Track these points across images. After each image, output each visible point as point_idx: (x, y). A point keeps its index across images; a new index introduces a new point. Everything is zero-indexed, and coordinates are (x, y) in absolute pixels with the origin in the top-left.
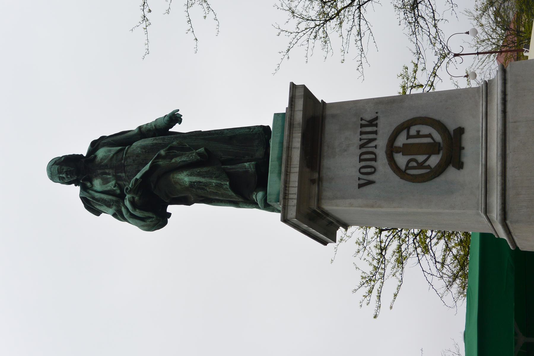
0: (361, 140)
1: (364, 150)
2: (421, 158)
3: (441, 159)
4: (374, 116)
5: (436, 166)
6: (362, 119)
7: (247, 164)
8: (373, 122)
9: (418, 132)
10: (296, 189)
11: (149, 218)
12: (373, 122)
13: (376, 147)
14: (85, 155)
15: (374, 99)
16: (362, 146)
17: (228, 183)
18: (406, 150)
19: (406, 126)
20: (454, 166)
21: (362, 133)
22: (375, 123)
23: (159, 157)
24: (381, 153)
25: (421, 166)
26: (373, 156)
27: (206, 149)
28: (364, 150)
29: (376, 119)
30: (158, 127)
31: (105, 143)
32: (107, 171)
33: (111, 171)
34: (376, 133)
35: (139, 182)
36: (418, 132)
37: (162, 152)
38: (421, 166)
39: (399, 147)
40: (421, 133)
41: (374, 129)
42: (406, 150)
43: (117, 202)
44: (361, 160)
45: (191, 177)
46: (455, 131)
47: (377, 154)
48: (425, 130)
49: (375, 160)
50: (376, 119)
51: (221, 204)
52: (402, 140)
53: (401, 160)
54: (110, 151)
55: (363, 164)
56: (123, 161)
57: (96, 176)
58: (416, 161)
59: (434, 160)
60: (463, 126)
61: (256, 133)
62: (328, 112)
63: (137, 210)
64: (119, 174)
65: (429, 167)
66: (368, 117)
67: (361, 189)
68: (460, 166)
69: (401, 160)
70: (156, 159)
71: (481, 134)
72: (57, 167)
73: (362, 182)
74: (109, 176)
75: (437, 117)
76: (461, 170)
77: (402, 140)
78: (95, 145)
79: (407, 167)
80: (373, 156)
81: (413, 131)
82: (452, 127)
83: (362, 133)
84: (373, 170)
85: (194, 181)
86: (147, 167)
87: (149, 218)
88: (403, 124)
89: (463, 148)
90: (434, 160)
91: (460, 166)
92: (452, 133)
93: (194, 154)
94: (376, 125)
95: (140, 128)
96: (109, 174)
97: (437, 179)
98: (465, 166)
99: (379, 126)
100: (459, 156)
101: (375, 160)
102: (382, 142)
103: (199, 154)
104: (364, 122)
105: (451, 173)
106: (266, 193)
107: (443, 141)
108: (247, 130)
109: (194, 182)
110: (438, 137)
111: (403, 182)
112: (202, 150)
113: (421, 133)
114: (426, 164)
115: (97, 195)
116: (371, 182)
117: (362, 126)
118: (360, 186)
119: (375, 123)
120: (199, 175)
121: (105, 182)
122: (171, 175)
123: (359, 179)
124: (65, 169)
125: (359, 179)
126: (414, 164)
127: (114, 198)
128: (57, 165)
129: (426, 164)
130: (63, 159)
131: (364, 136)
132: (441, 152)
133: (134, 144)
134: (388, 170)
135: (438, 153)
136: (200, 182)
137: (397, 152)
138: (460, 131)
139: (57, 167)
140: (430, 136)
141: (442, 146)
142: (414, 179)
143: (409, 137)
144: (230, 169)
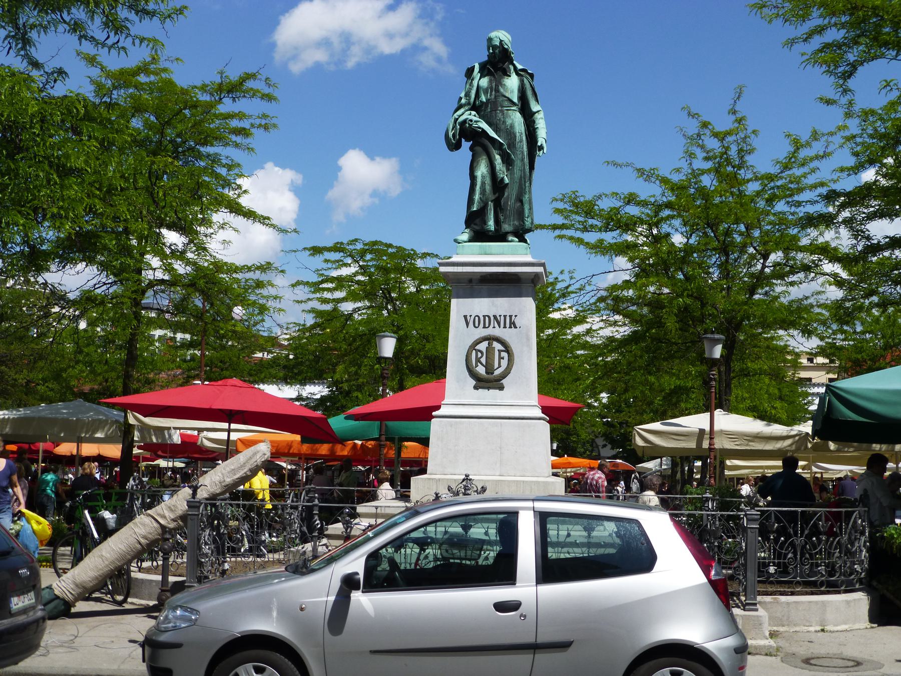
1: (492, 318)
2: (483, 360)
3: (481, 374)
6: (516, 316)
8: (513, 325)
12: (513, 325)
16: (495, 317)
18: (490, 349)
19: (507, 349)
21: (505, 316)
24: (489, 332)
25: (478, 360)
26: (487, 326)
28: (492, 318)
29: (516, 327)
30: (537, 130)
32: (494, 92)
33: (493, 97)
34: (505, 327)
36: (503, 358)
38: (478, 360)
41: (508, 325)
42: (490, 349)
43: (469, 104)
44: (484, 316)
48: (504, 363)
49: (484, 327)
50: (516, 327)
52: (497, 346)
53: (483, 346)
54: (512, 92)
59: (481, 370)
65: (477, 366)
66: (518, 322)
68: (476, 388)
69: (483, 346)
71: (499, 402)
73: (468, 318)
80: (487, 326)
81: (504, 354)
86: (493, 134)
90: (481, 370)
93: (502, 176)
94: (510, 327)
96: (491, 95)
101: (484, 327)
102: (497, 332)
103: (503, 179)
104: (513, 318)
110: (497, 372)
112: (507, 180)
115: (475, 83)
117: (511, 316)
118: (465, 317)
120: (483, 184)
122: (484, 157)
123: (471, 316)
126: (479, 355)
131: (502, 318)
138: (501, 388)
140: (500, 366)
143: (500, 351)
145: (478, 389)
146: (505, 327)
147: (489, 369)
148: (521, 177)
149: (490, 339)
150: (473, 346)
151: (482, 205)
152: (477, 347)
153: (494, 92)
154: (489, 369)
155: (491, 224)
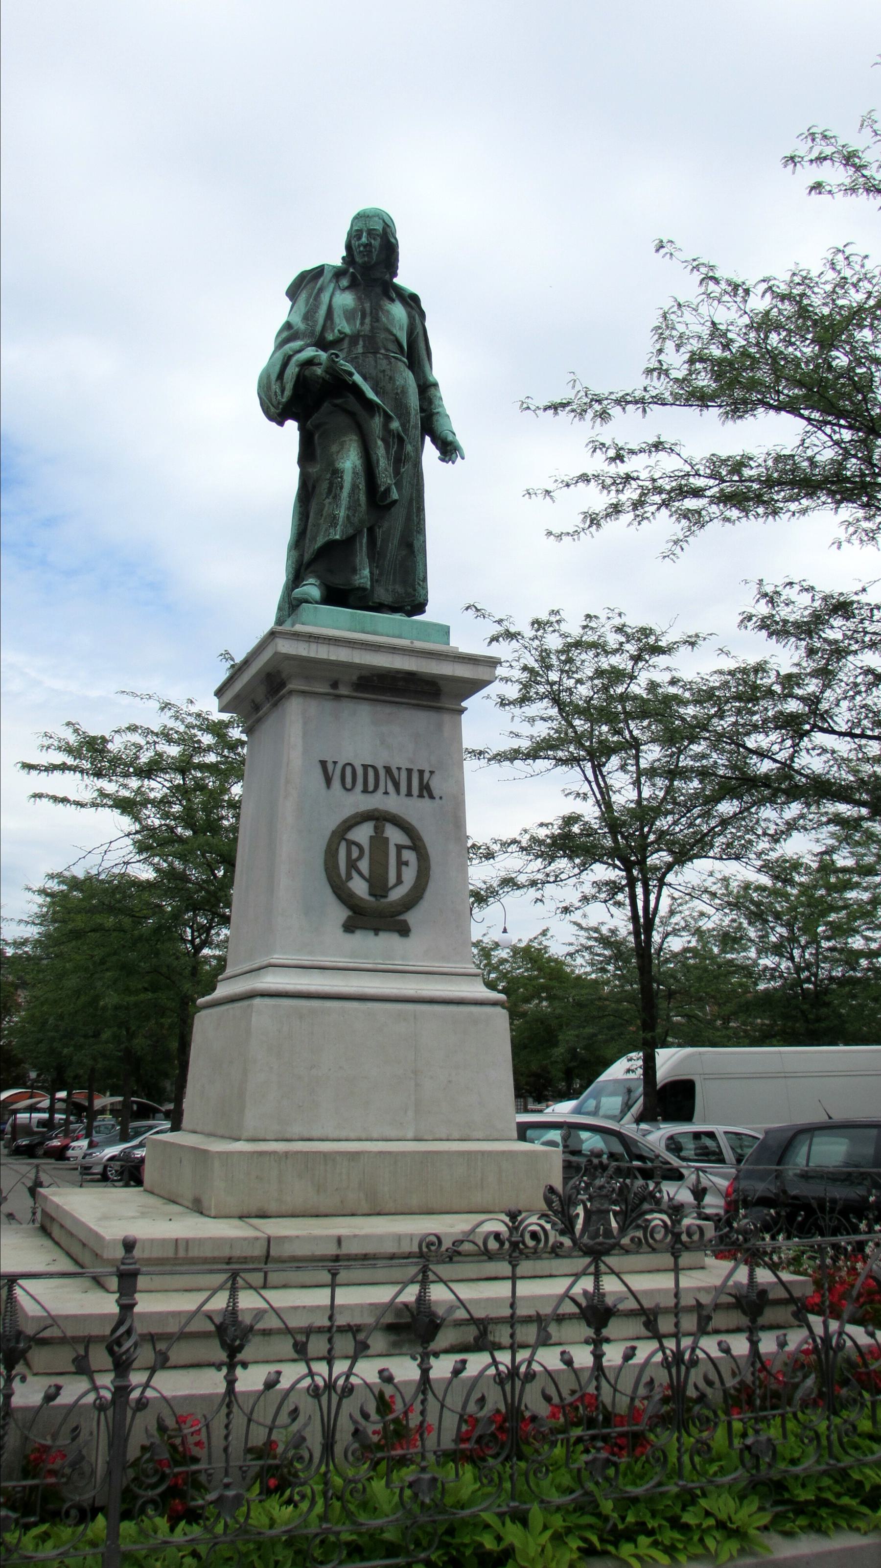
0: (399, 769)
1: (382, 773)
2: (364, 866)
3: (361, 899)
4: (436, 793)
5: (350, 889)
6: (432, 772)
7: (366, 572)
8: (426, 790)
9: (406, 864)
10: (325, 657)
11: (283, 391)
12: (426, 790)
13: (386, 793)
14: (395, 280)
15: (463, 794)
16: (388, 770)
17: (338, 537)
18: (379, 842)
19: (417, 844)
20: (349, 918)
21: (409, 771)
22: (425, 794)
23: (388, 418)
25: (352, 865)
26: (371, 787)
27: (395, 501)
28: (382, 773)
29: (432, 797)
30: (435, 418)
31: (414, 320)
32: (368, 320)
33: (367, 327)
34: (409, 794)
35: (347, 378)
36: (406, 864)
37: (395, 425)
38: (352, 865)
39: (383, 832)
40: (404, 868)
42: (379, 842)
43: (312, 333)
44: (365, 767)
45: (351, 471)
46: (405, 922)
47: (374, 794)
48: (409, 875)
49: (365, 791)
50: (432, 797)
51: (297, 518)
52: (395, 836)
53: (363, 834)
54: (401, 328)
55: (360, 772)
56: (383, 351)
57: (359, 299)
58: (360, 857)
59: (359, 887)
60: (413, 934)
61: (415, 590)
62: (447, 718)
63: (297, 369)
64: (361, 343)
65: (349, 877)
66: (436, 784)
67: (319, 766)
68: (349, 927)
69: (363, 834)
70: (385, 413)
71: (398, 963)
72: (379, 227)
73: (330, 767)
74: (358, 322)
75: (428, 895)
76: (342, 930)
77: (395, 836)
78: (412, 302)
79: (351, 843)
80: (371, 787)
81: (409, 856)
82: (412, 918)
83: (409, 771)
84: (349, 786)
85: (345, 477)
86: (371, 395)
87: (283, 391)
88: (420, 839)
89: (376, 934)
90: (359, 887)
91: (349, 927)
92: (401, 917)
94: (421, 796)
95: (435, 385)
96: (362, 324)
97: (328, 891)
98: (348, 936)
99: (420, 799)
100: (364, 928)
101: (365, 791)
102: (393, 803)
103: (388, 490)
104: (426, 775)
105: (340, 914)
106: (317, 603)
107: (391, 904)
108: (421, 576)
109: (342, 477)
110: (396, 895)
111: (328, 834)
112: (395, 495)
113: (404, 868)
114: (355, 874)
115: (325, 298)
116: (328, 781)
117: (421, 772)
118: (323, 764)
119: (425, 794)
120: (354, 487)
121: (349, 315)
122: (354, 437)
123: (335, 763)
124: (376, 243)
125: (335, 763)
126: (355, 854)
127: (319, 328)
128: (384, 229)
129: (355, 874)
130: (393, 240)
131: (404, 775)
132: (372, 899)
133: (411, 374)
134: (348, 811)
135: (371, 894)
136: (342, 488)
137: (376, 828)
138: (404, 931)
139: (379, 227)
140: (399, 881)
141: (383, 900)
142: (331, 854)
143: (399, 848)
144: (361, 543)
145: (352, 932)
146: (409, 794)
147: (379, 887)
148: (411, 500)
149: (379, 818)
150: (342, 832)
151: (351, 531)
152: (353, 835)
153: (368, 320)
154: (379, 887)
155: (364, 576)
